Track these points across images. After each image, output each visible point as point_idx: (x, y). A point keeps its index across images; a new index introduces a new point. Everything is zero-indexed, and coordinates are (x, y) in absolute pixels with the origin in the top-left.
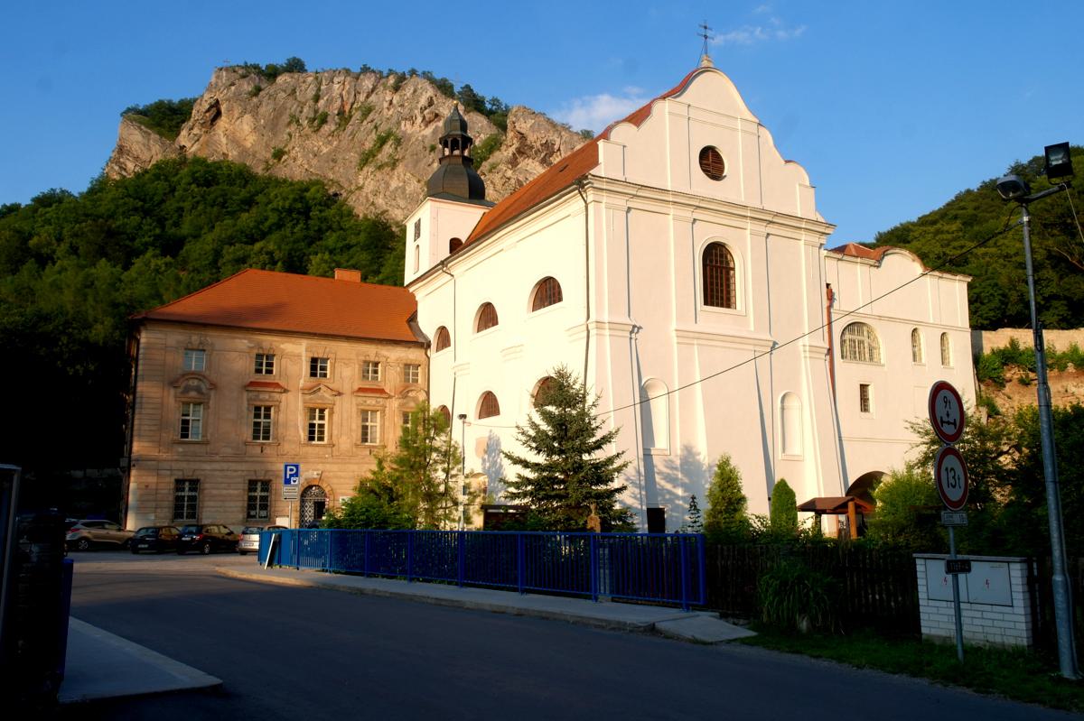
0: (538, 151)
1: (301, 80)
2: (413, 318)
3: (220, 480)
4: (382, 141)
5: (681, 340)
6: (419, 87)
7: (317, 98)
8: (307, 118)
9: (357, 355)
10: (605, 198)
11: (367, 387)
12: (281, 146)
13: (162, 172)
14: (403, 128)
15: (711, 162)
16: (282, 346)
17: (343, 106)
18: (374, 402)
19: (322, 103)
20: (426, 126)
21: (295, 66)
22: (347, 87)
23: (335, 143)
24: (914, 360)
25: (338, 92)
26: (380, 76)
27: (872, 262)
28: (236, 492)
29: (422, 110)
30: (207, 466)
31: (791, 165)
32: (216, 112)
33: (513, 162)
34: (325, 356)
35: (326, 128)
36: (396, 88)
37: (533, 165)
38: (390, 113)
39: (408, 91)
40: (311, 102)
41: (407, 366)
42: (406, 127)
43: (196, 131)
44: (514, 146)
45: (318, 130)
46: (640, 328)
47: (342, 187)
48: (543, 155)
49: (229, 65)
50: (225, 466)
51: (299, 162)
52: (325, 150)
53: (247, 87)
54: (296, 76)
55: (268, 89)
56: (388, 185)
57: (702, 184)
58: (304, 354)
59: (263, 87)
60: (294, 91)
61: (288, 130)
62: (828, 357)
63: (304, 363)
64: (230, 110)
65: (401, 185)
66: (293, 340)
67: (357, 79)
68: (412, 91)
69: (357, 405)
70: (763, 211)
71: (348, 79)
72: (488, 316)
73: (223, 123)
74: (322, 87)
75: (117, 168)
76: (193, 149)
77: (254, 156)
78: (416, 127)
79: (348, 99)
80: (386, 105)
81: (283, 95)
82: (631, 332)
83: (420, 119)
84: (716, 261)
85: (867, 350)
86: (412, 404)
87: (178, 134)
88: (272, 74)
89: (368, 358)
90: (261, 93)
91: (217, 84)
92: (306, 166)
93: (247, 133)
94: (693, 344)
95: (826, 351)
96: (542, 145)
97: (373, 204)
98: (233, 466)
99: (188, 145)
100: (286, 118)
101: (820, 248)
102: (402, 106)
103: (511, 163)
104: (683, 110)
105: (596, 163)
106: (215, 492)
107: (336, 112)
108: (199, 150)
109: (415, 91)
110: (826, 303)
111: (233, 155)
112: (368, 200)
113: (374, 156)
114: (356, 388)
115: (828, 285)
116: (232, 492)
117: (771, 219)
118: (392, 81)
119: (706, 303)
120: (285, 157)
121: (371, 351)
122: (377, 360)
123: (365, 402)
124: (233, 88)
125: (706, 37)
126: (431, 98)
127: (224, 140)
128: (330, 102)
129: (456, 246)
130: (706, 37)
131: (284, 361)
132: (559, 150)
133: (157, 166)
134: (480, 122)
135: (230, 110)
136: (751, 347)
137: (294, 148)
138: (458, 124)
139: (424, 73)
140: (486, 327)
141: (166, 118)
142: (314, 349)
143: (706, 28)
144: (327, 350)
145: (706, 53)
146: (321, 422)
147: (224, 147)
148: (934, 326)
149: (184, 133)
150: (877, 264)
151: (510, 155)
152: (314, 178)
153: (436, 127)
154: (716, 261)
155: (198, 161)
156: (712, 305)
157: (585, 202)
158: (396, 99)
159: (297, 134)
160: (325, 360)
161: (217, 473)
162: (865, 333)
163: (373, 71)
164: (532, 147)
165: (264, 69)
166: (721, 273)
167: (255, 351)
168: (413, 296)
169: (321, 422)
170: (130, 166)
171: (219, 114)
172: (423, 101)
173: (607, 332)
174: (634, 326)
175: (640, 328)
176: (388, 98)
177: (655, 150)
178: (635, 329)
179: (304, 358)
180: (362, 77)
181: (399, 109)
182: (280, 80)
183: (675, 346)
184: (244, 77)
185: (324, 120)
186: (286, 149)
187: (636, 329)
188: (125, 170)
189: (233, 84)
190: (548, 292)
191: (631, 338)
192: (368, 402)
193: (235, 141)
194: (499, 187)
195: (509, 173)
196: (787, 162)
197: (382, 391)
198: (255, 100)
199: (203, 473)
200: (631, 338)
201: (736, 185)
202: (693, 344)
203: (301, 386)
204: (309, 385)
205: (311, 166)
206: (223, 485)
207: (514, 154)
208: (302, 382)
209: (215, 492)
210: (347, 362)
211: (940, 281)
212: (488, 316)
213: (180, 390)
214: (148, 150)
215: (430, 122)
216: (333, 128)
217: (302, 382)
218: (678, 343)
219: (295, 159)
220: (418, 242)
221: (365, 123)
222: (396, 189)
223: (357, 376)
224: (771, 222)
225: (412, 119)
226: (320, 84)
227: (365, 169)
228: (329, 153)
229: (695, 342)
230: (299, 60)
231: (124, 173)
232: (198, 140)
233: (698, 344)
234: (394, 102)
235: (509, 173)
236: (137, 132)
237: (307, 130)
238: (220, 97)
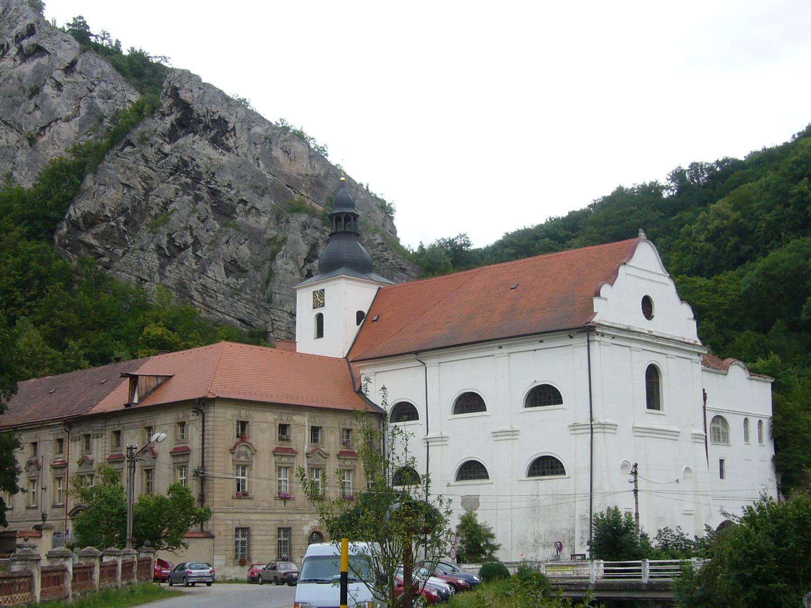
0: (207, 127)
16: (294, 418)
20: (24, 60)
28: (270, 538)
29: (18, 39)
30: (254, 517)
33: (172, 136)
37: (201, 143)
44: (173, 117)
48: (213, 133)
63: (307, 431)
83: (13, 51)
96: (213, 121)
98: (269, 517)
103: (169, 136)
106: (259, 538)
116: (268, 537)
134: (100, 66)
151: (168, 126)
153: (38, 64)
164: (200, 122)
167: (279, 422)
195: (167, 148)
197: (353, 454)
199: (251, 522)
203: (306, 450)
204: (311, 449)
206: (263, 533)
207: (172, 125)
209: (259, 538)
213: (235, 455)
217: (306, 447)
235: (167, 148)
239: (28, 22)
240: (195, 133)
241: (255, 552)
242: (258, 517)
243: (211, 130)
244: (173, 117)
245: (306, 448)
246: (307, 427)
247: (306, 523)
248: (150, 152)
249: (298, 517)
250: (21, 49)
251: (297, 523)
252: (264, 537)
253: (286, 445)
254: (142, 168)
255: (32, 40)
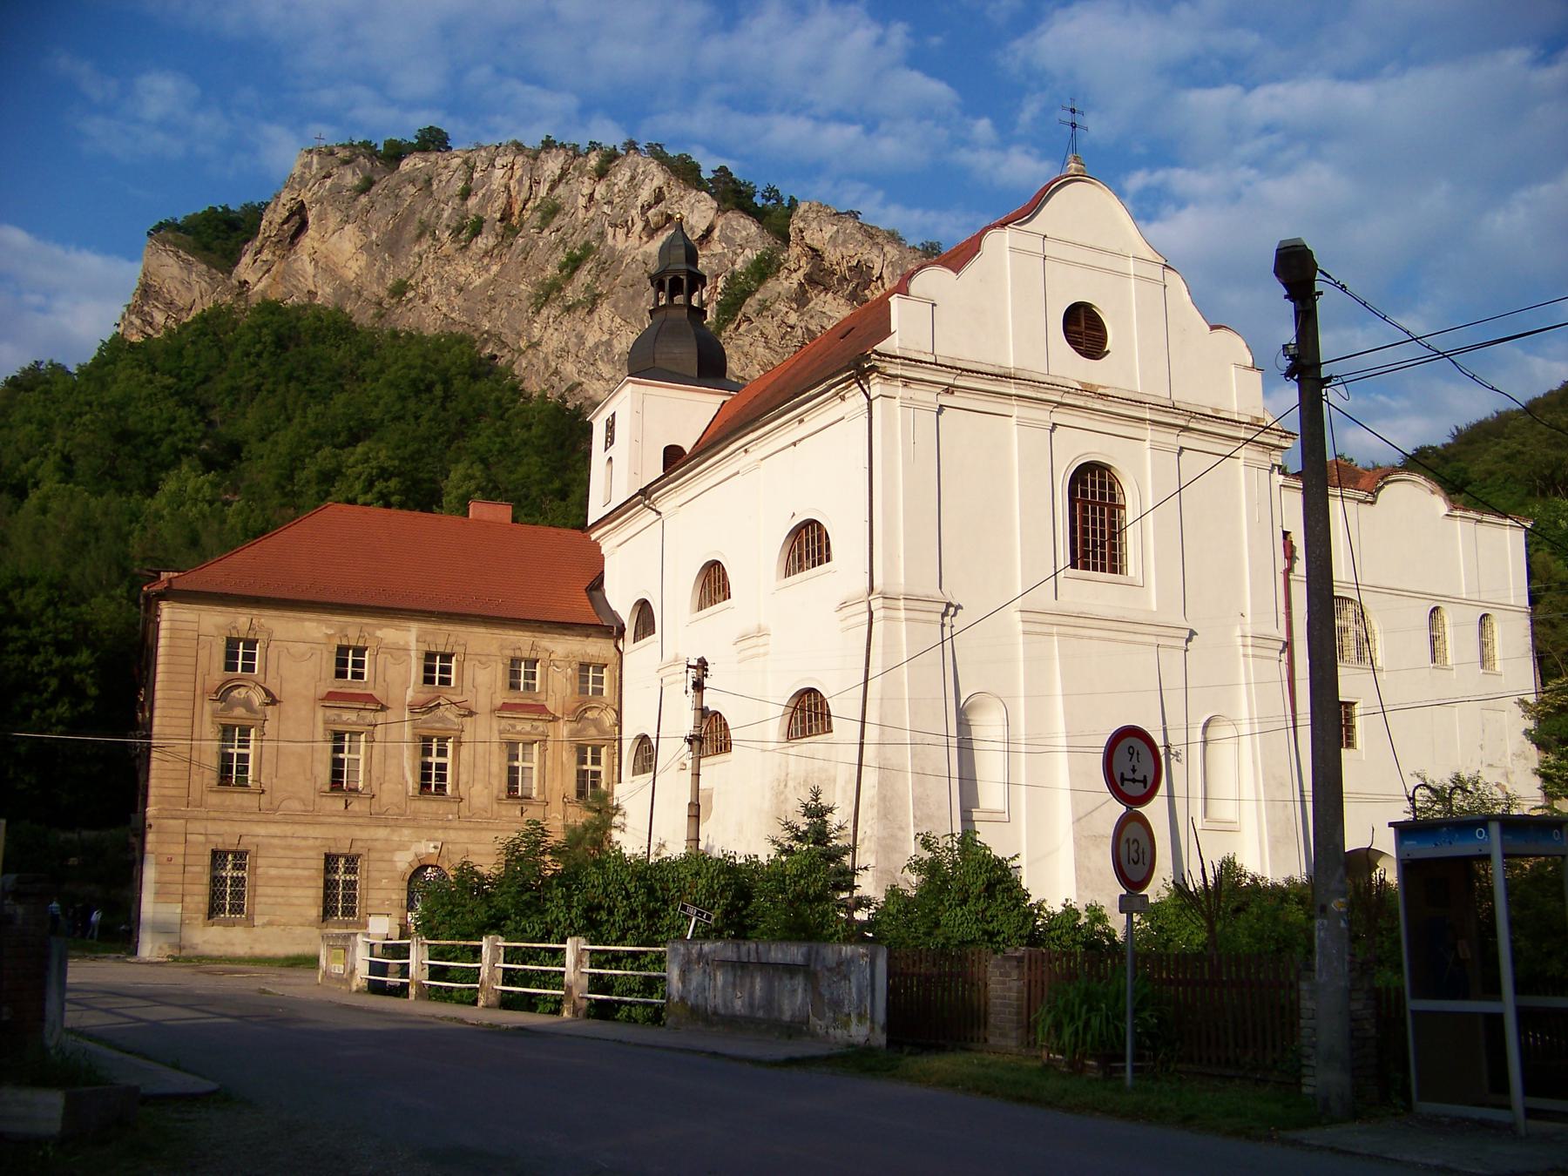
1: (442, 163)
2: (596, 584)
3: (281, 853)
4: (573, 264)
5: (1030, 627)
6: (640, 170)
7: (466, 194)
8: (448, 227)
9: (502, 648)
10: (898, 390)
11: (518, 701)
12: (404, 276)
13: (211, 325)
14: (610, 241)
15: (1084, 329)
16: (379, 633)
17: (510, 205)
18: (528, 728)
19: (472, 202)
21: (434, 141)
22: (518, 173)
23: (495, 269)
24: (1434, 660)
25: (503, 181)
26: (576, 152)
27: (1361, 495)
28: (306, 873)
29: (645, 208)
30: (261, 830)
31: (1222, 332)
32: (298, 221)
33: (800, 299)
34: (448, 651)
35: (484, 242)
36: (602, 173)
37: (835, 304)
38: (591, 214)
39: (621, 177)
40: (457, 200)
41: (584, 667)
42: (618, 241)
43: (266, 255)
44: (801, 273)
45: (466, 247)
46: (958, 607)
47: (504, 345)
48: (852, 285)
49: (323, 143)
50: (288, 829)
51: (432, 303)
52: (478, 282)
53: (351, 178)
54: (433, 157)
55: (386, 182)
56: (581, 339)
57: (1070, 365)
58: (413, 645)
59: (376, 178)
60: (429, 182)
61: (416, 249)
62: (1285, 656)
63: (414, 661)
64: (321, 218)
65: (605, 338)
66: (396, 622)
67: (535, 159)
68: (627, 178)
69: (500, 732)
70: (1173, 409)
71: (520, 160)
72: (714, 582)
73: (308, 241)
74: (476, 175)
75: (138, 322)
76: (260, 286)
77: (359, 294)
78: (634, 240)
79: (519, 193)
80: (582, 201)
81: (411, 189)
82: (944, 615)
83: (639, 225)
84: (1093, 495)
85: (1353, 644)
86: (592, 731)
87: (236, 263)
88: (395, 154)
89: (518, 654)
90: (374, 189)
91: (302, 176)
92: (444, 310)
93: (348, 255)
94: (1051, 634)
95: (1281, 645)
96: (850, 269)
97: (556, 372)
98: (300, 830)
99: (251, 279)
100: (412, 229)
101: (1271, 471)
102: (610, 203)
103: (796, 300)
104: (1035, 244)
105: (887, 333)
106: (273, 872)
107: (498, 216)
108: (270, 286)
109: (633, 178)
110: (1282, 564)
111: (325, 294)
112: (547, 366)
113: (560, 289)
114: (499, 702)
115: (1286, 534)
116: (299, 872)
117: (1184, 420)
118: (594, 160)
119: (1074, 565)
120: (411, 294)
121: (522, 641)
122: (533, 655)
123: (514, 726)
124: (328, 182)
125: (1074, 126)
126: (660, 188)
127: (310, 269)
128: (489, 198)
129: (674, 458)
130: (1074, 126)
131: (381, 658)
132: (880, 277)
133: (203, 318)
134: (745, 228)
135: (321, 218)
136: (1153, 639)
137: (425, 278)
138: (682, 251)
139: (649, 146)
140: (713, 602)
141: (219, 235)
142: (429, 638)
143: (1073, 111)
144: (452, 639)
145: (1074, 150)
146: (441, 760)
147: (310, 280)
148: (1467, 602)
149: (246, 259)
150: (1370, 499)
152: (457, 329)
154: (1093, 495)
155: (271, 308)
156: (1085, 567)
157: (868, 397)
158: (601, 189)
159: (431, 256)
160: (447, 657)
161: (276, 841)
162: (1351, 615)
163: (563, 146)
164: (834, 273)
165: (381, 147)
166: (1102, 513)
167: (337, 642)
168: (596, 546)
169: (441, 760)
170: (159, 318)
171: (303, 226)
172: (645, 194)
173: (902, 614)
174: (949, 605)
175: (958, 607)
176: (586, 191)
177: (987, 306)
178: (951, 609)
179: (413, 654)
180: (543, 155)
181: (606, 209)
182: (407, 165)
183: (1021, 638)
184: (345, 162)
185: (477, 231)
186: (412, 282)
187: (952, 610)
188: (150, 324)
189: (328, 176)
190: (808, 545)
191: (943, 625)
192: (519, 728)
193: (328, 269)
194: (775, 342)
195: (793, 318)
196: (1212, 328)
197: (542, 709)
198: (364, 199)
199: (255, 840)
200: (943, 625)
201: (1128, 365)
202: (1051, 634)
203: (408, 699)
204: (422, 697)
205: (453, 310)
206: (286, 862)
207: (801, 284)
208: (410, 692)
209: (273, 872)
210: (483, 659)
211: (1479, 526)
212: (714, 582)
214: (190, 288)
215: (657, 229)
216: (492, 242)
217: (410, 692)
218: (1025, 633)
219: (426, 299)
220: (612, 451)
221: (546, 233)
222: (597, 346)
223: (499, 684)
224: (1186, 429)
225: (628, 227)
226: (473, 169)
227: (545, 312)
228: (487, 284)
229: (1055, 629)
230: (439, 131)
231: (151, 331)
232: (268, 270)
233: (1059, 634)
234: (597, 196)
235: (793, 318)
236: (171, 261)
237: (449, 247)
238: (306, 196)
239: (656, 183)
240: (827, 290)
241: (263, 900)
242: (274, 829)
243: (849, 282)
244: (801, 273)
245: (410, 695)
246: (413, 654)
247: (403, 847)
248: (771, 328)
249: (382, 833)
250: (647, 222)
251: (378, 845)
252: (288, 872)
253: (349, 685)
254: (761, 350)
255: (661, 207)
